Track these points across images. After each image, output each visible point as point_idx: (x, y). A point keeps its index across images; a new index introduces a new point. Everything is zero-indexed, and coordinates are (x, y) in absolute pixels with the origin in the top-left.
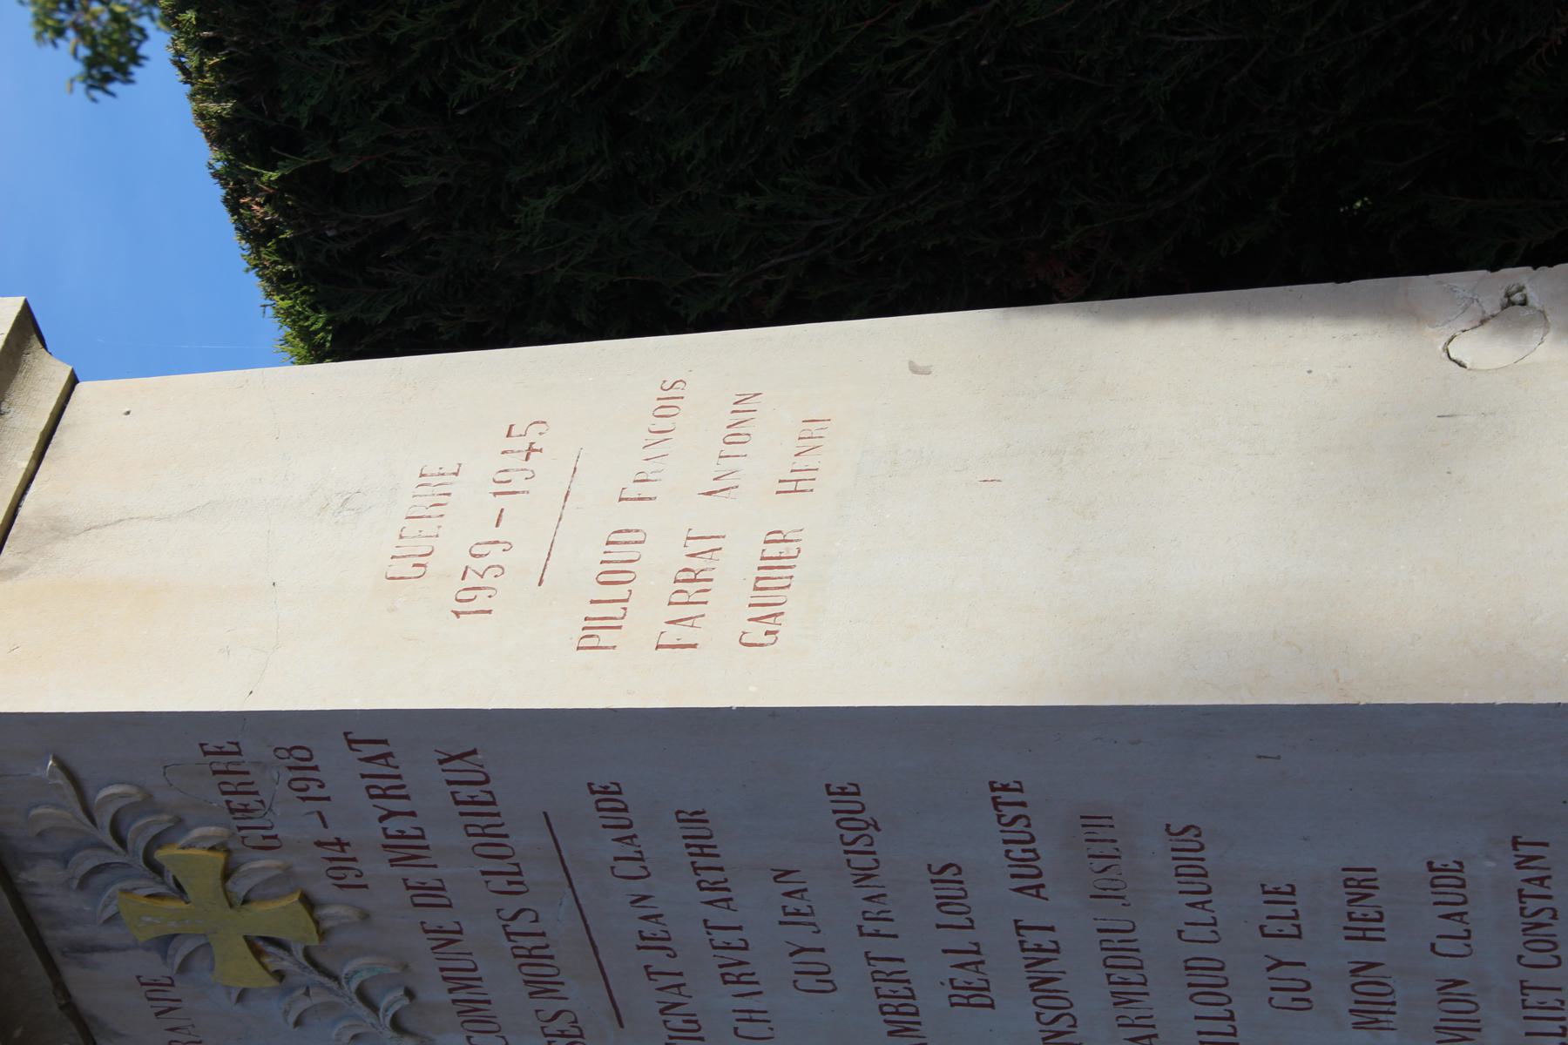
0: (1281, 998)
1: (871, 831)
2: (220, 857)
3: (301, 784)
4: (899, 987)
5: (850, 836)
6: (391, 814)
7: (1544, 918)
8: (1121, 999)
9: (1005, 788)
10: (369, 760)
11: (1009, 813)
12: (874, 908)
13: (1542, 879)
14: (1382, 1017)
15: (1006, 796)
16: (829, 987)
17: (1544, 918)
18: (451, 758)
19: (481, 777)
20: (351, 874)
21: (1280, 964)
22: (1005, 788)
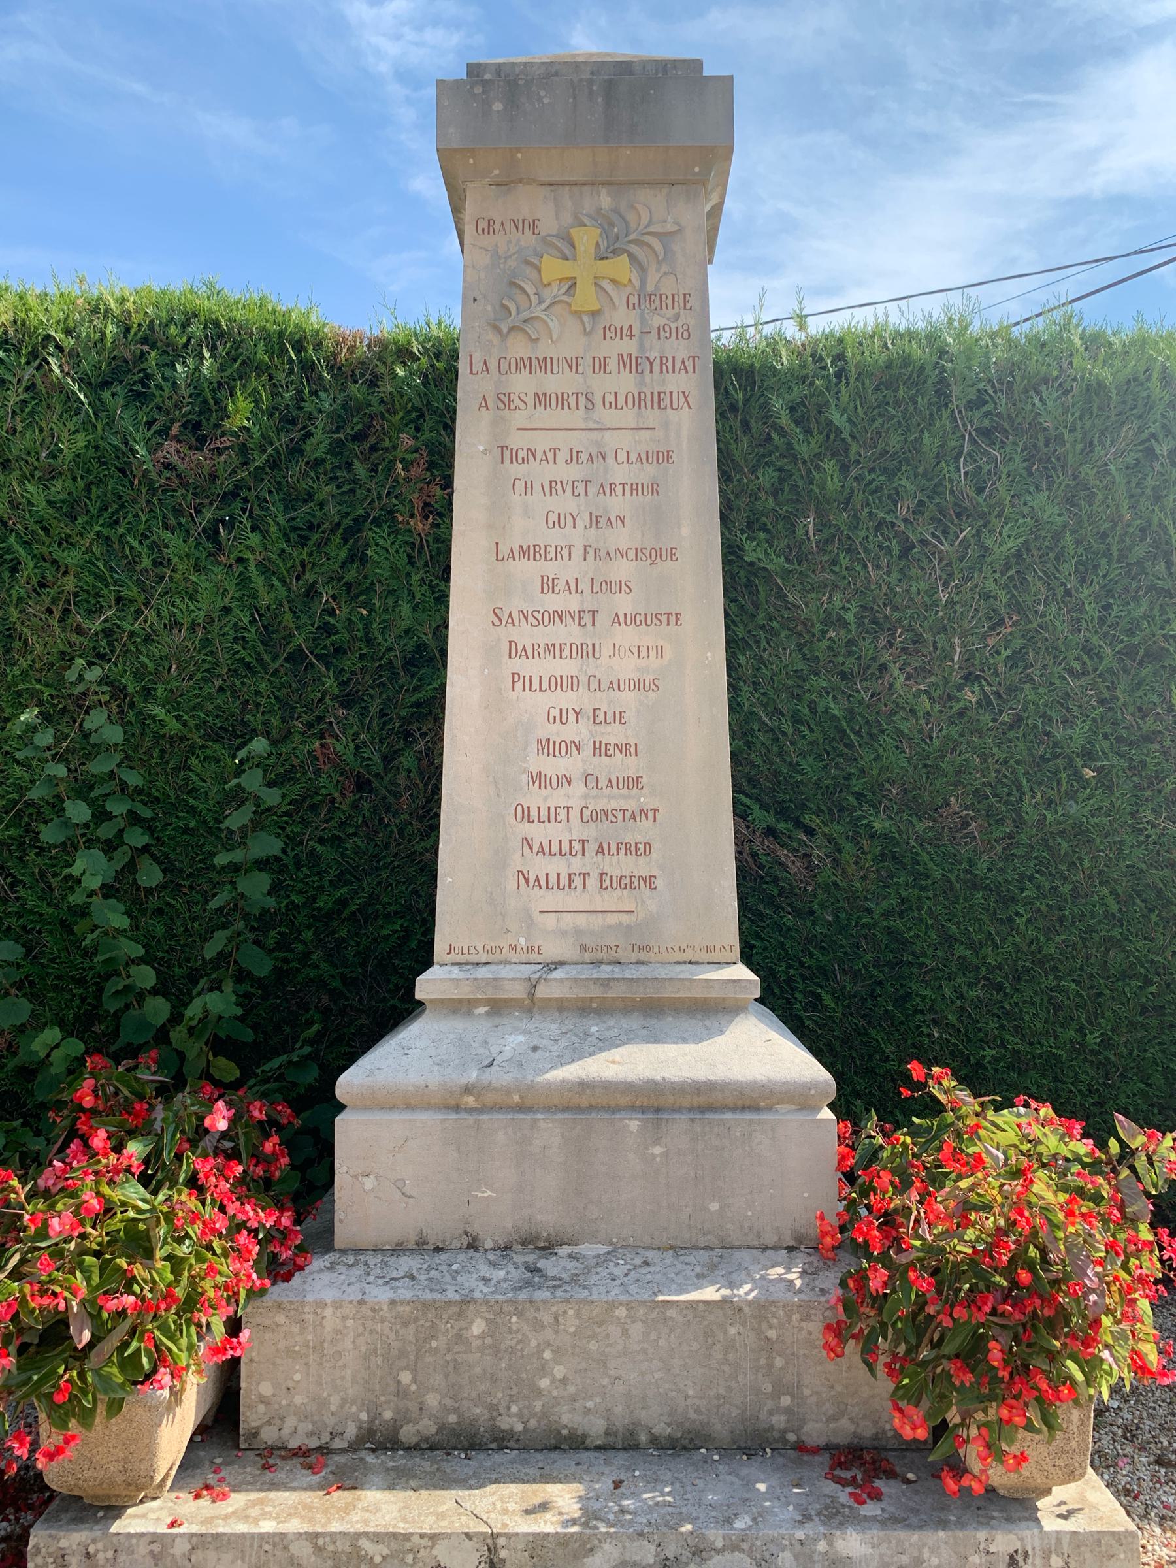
0: (555, 713)
1: (649, 561)
2: (626, 282)
3: (667, 329)
4: (553, 555)
5: (647, 553)
6: (651, 364)
7: (611, 817)
8: (550, 648)
9: (677, 619)
10: (683, 362)
11: (664, 619)
12: (603, 554)
13: (634, 819)
14: (546, 751)
15: (672, 619)
16: (551, 525)
17: (611, 817)
18: (686, 398)
19: (675, 406)
20: (613, 335)
21: (577, 714)
22: (677, 619)
